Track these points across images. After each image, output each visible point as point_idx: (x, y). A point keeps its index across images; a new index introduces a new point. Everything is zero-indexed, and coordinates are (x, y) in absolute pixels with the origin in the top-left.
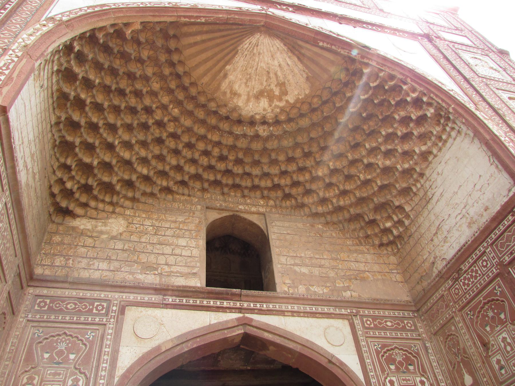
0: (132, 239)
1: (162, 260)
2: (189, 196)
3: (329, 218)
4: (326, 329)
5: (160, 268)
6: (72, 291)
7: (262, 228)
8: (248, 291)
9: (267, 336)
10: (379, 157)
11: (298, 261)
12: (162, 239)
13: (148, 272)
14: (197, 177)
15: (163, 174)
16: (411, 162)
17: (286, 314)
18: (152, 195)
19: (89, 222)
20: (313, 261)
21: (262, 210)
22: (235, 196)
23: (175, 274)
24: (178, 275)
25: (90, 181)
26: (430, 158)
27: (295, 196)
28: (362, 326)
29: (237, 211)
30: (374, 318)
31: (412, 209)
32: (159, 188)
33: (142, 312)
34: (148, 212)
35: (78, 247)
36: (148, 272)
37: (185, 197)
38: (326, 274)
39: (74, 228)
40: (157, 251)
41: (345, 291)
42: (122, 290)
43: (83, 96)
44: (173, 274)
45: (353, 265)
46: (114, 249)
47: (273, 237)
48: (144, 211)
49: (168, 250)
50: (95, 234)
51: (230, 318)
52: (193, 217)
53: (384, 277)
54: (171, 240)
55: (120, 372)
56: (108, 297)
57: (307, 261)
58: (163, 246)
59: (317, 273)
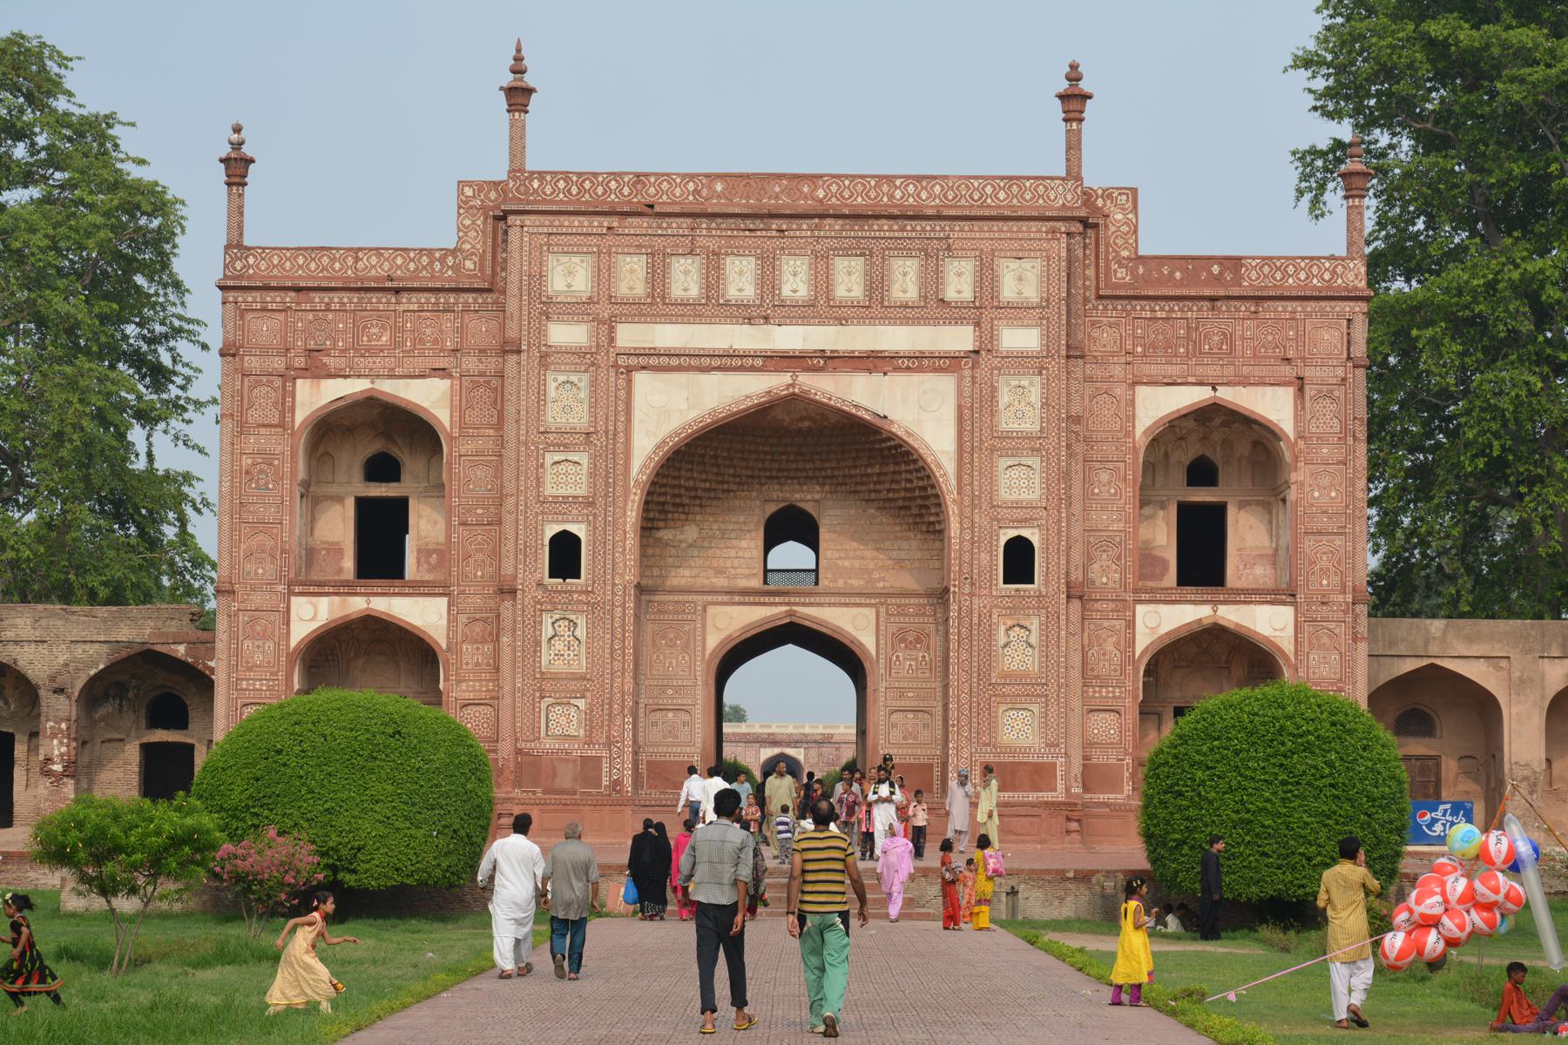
9: (807, 623)
14: (752, 477)
15: (722, 482)
21: (817, 497)
30: (899, 606)
48: (712, 514)
49: (733, 553)
55: (708, 652)
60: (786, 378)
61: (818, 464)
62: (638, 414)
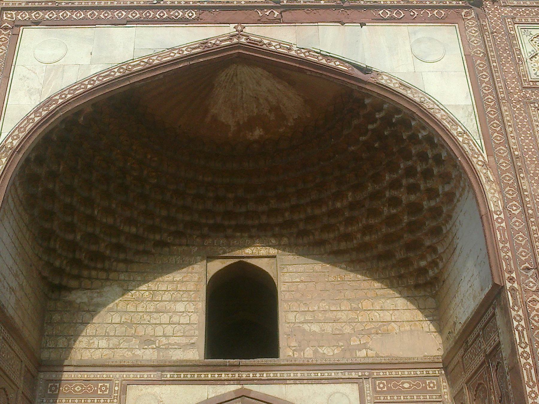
0: (128, 310)
1: (159, 331)
2: (187, 245)
3: (354, 255)
4: (330, 396)
5: (158, 341)
6: (77, 373)
7: (272, 275)
8: (247, 360)
10: (402, 190)
11: (309, 317)
12: (160, 305)
13: (146, 347)
16: (438, 200)
17: (288, 382)
18: (146, 252)
19: (85, 293)
20: (327, 316)
22: (242, 237)
23: (173, 347)
24: (176, 347)
25: (77, 256)
26: (455, 201)
27: (313, 231)
28: (373, 390)
29: (243, 257)
31: (444, 252)
32: (153, 242)
33: (142, 390)
34: (143, 272)
35: (78, 325)
36: (146, 347)
37: (183, 247)
38: (340, 330)
39: (71, 303)
40: (154, 322)
41: (360, 350)
42: (122, 369)
43: (51, 186)
44: (170, 347)
45: (376, 316)
46: (111, 323)
47: (283, 289)
49: (165, 318)
50: (91, 308)
51: (228, 390)
52: (191, 273)
53: (413, 328)
54: (168, 306)
56: (110, 377)
57: (320, 315)
58: (161, 314)
59: (329, 330)
60: (231, 29)
61: (273, 204)
62: (20, 70)
